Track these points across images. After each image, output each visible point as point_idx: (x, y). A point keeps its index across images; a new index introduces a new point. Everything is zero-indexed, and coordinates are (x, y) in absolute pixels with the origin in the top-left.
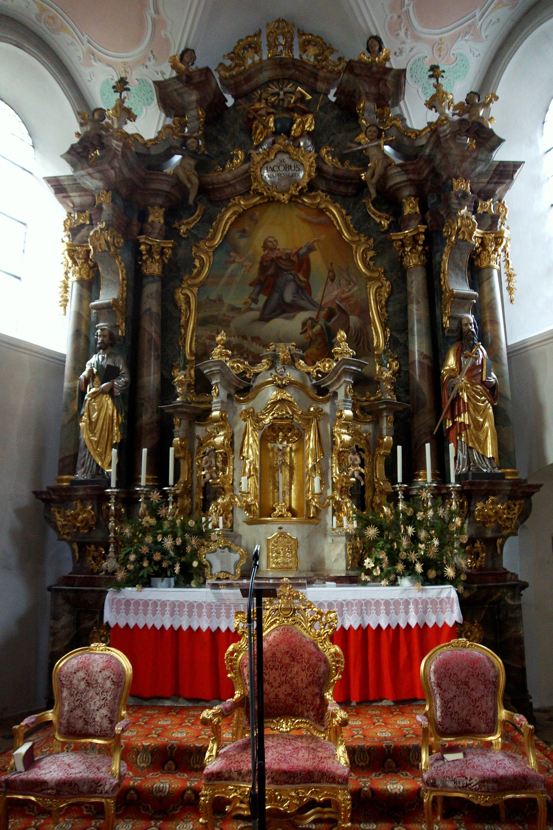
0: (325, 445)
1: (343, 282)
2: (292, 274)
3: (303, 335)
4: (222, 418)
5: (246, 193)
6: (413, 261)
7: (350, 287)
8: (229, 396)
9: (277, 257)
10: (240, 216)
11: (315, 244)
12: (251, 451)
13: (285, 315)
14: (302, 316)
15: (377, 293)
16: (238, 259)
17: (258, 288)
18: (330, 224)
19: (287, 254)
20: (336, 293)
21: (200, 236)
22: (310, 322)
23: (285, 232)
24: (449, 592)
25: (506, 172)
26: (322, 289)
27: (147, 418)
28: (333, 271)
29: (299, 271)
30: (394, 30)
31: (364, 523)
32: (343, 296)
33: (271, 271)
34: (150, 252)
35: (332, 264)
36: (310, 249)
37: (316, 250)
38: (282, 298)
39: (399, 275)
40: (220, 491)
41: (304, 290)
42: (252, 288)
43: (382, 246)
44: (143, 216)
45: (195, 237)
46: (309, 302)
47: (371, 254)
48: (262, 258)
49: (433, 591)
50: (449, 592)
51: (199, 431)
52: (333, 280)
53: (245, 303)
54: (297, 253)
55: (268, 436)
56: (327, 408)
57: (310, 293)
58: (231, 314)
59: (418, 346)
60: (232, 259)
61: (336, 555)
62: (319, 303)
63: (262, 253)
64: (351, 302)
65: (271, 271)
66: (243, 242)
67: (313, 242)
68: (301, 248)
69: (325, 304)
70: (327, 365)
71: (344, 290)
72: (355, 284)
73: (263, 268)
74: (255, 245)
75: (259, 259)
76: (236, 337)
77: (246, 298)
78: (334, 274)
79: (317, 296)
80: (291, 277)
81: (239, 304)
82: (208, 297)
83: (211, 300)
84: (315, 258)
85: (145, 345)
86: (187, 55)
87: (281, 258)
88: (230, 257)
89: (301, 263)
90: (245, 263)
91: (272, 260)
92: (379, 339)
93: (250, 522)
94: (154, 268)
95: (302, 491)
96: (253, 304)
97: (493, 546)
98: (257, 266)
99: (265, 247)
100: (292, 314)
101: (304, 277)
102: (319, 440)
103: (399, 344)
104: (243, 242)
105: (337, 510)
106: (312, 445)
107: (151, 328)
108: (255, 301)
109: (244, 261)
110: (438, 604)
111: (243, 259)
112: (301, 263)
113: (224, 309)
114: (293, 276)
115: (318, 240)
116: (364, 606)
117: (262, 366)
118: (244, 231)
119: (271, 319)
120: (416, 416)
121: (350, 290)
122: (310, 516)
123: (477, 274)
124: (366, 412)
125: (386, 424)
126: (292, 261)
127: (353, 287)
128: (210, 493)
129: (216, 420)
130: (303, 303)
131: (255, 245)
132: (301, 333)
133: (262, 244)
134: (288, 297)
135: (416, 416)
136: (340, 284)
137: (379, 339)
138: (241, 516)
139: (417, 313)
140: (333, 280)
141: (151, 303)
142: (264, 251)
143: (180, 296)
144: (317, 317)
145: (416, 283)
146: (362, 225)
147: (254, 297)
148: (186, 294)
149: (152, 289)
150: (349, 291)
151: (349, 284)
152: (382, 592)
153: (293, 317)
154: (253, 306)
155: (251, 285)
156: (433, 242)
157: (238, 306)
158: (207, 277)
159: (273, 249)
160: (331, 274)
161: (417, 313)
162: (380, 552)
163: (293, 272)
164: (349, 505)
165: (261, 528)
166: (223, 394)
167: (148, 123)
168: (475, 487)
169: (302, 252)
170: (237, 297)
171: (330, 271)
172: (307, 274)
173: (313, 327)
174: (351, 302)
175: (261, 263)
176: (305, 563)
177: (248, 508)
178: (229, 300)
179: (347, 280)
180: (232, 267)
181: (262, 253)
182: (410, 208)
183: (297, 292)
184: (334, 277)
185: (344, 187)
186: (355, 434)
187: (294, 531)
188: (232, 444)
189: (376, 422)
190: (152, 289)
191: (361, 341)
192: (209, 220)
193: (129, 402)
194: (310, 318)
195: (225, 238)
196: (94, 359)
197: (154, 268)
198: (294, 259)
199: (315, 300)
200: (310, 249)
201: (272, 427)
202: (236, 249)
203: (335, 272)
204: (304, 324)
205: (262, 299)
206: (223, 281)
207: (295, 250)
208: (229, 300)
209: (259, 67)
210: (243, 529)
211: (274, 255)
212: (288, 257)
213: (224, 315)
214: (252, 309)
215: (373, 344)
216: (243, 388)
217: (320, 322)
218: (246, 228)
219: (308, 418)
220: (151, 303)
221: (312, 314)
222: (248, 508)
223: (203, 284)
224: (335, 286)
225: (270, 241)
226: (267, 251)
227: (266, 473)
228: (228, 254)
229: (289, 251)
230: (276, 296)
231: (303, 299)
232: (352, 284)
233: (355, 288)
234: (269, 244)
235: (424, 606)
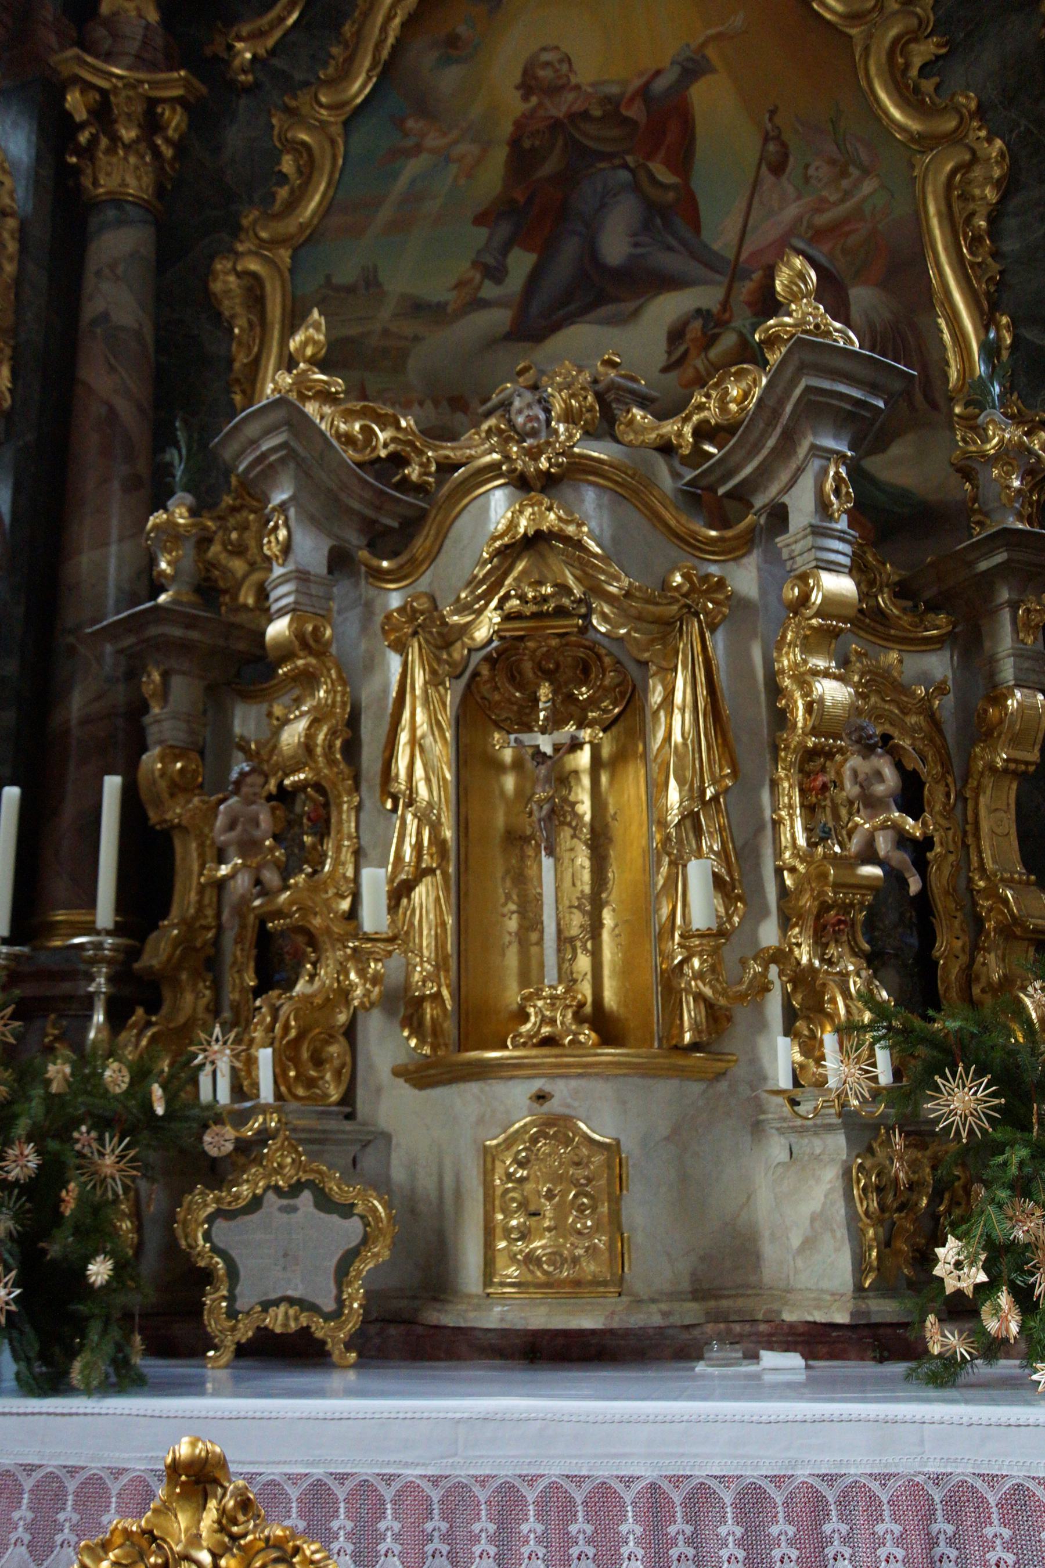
0: (744, 729)
1: (820, 170)
2: (625, 166)
3: (673, 376)
4: (305, 642)
7: (845, 183)
8: (340, 561)
9: (572, 117)
11: (711, 52)
13: (604, 311)
14: (668, 308)
15: (956, 195)
16: (433, 141)
17: (504, 229)
19: (607, 100)
20: (792, 211)
21: (299, 76)
22: (697, 324)
26: (741, 204)
28: (778, 138)
29: (649, 157)
31: (925, 1060)
32: (822, 220)
33: (549, 167)
34: (103, 113)
35: (773, 113)
36: (693, 69)
37: (712, 70)
38: (591, 251)
41: (673, 215)
42: (483, 232)
45: (285, 76)
46: (693, 255)
47: (923, 51)
48: (518, 125)
52: (778, 169)
53: (460, 285)
54: (644, 92)
55: (491, 695)
56: (745, 578)
57: (697, 227)
58: (409, 328)
60: (409, 143)
61: (806, 1222)
62: (730, 255)
63: (515, 105)
64: (852, 240)
65: (549, 167)
66: (449, 80)
67: (704, 45)
68: (658, 73)
69: (753, 255)
71: (823, 200)
72: (866, 172)
73: (522, 158)
75: (506, 129)
76: (429, 404)
77: (462, 268)
78: (784, 145)
80: (624, 175)
81: (437, 289)
82: (328, 278)
83: (338, 289)
84: (713, 101)
85: (89, 441)
87: (585, 115)
88: (406, 135)
89: (661, 122)
90: (462, 148)
91: (556, 125)
93: (421, 1076)
94: (122, 175)
95: (647, 929)
96: (487, 283)
98: (500, 154)
99: (528, 86)
100: (631, 306)
101: (675, 172)
102: (714, 711)
104: (449, 80)
105: (804, 1013)
106: (679, 726)
108: (496, 273)
109: (456, 142)
111: (455, 134)
112: (661, 122)
113: (385, 313)
114: (631, 171)
115: (720, 36)
118: (453, 41)
119: (555, 328)
121: (847, 195)
126: (626, 121)
127: (857, 184)
128: (277, 957)
129: (286, 654)
130: (673, 262)
131: (494, 89)
132: (665, 370)
133: (517, 77)
134: (615, 246)
136: (807, 179)
138: (386, 1046)
140: (778, 169)
142: (526, 98)
143: (225, 282)
144: (725, 305)
147: (490, 261)
149: (119, 247)
150: (842, 200)
151: (844, 174)
153: (636, 313)
154: (489, 291)
155: (480, 220)
157: (435, 299)
158: (327, 209)
159: (554, 90)
160: (772, 147)
163: (630, 159)
164: (853, 984)
165: (464, 1099)
166: (311, 550)
169: (660, 85)
171: (766, 139)
172: (683, 160)
173: (711, 341)
174: (852, 240)
175: (515, 143)
176: (658, 1260)
177: (405, 1006)
178: (400, 281)
179: (833, 162)
180: (413, 167)
181: (515, 105)
183: (646, 226)
184: (786, 156)
186: (876, 684)
187: (603, 1113)
188: (352, 749)
189: (970, 643)
190: (119, 247)
194: (699, 312)
195: (388, 72)
197: (122, 175)
198: (635, 112)
199: (716, 247)
200: (693, 69)
201: (505, 655)
202: (424, 107)
203: (785, 137)
204: (676, 335)
205: (521, 263)
206: (385, 213)
207: (637, 83)
208: (400, 281)
210: (395, 1106)
211: (560, 108)
212: (612, 109)
213: (386, 332)
214: (482, 304)
215: (946, 378)
216: (389, 519)
217: (737, 323)
218: (462, 30)
219: (664, 623)
220: (116, 294)
221: (704, 297)
222: (405, 1006)
223: (310, 239)
224: (791, 190)
225: (547, 64)
226: (534, 100)
228: (399, 123)
229: (615, 90)
230: (570, 249)
231: (670, 248)
232: (855, 172)
233: (868, 187)
234: (541, 73)
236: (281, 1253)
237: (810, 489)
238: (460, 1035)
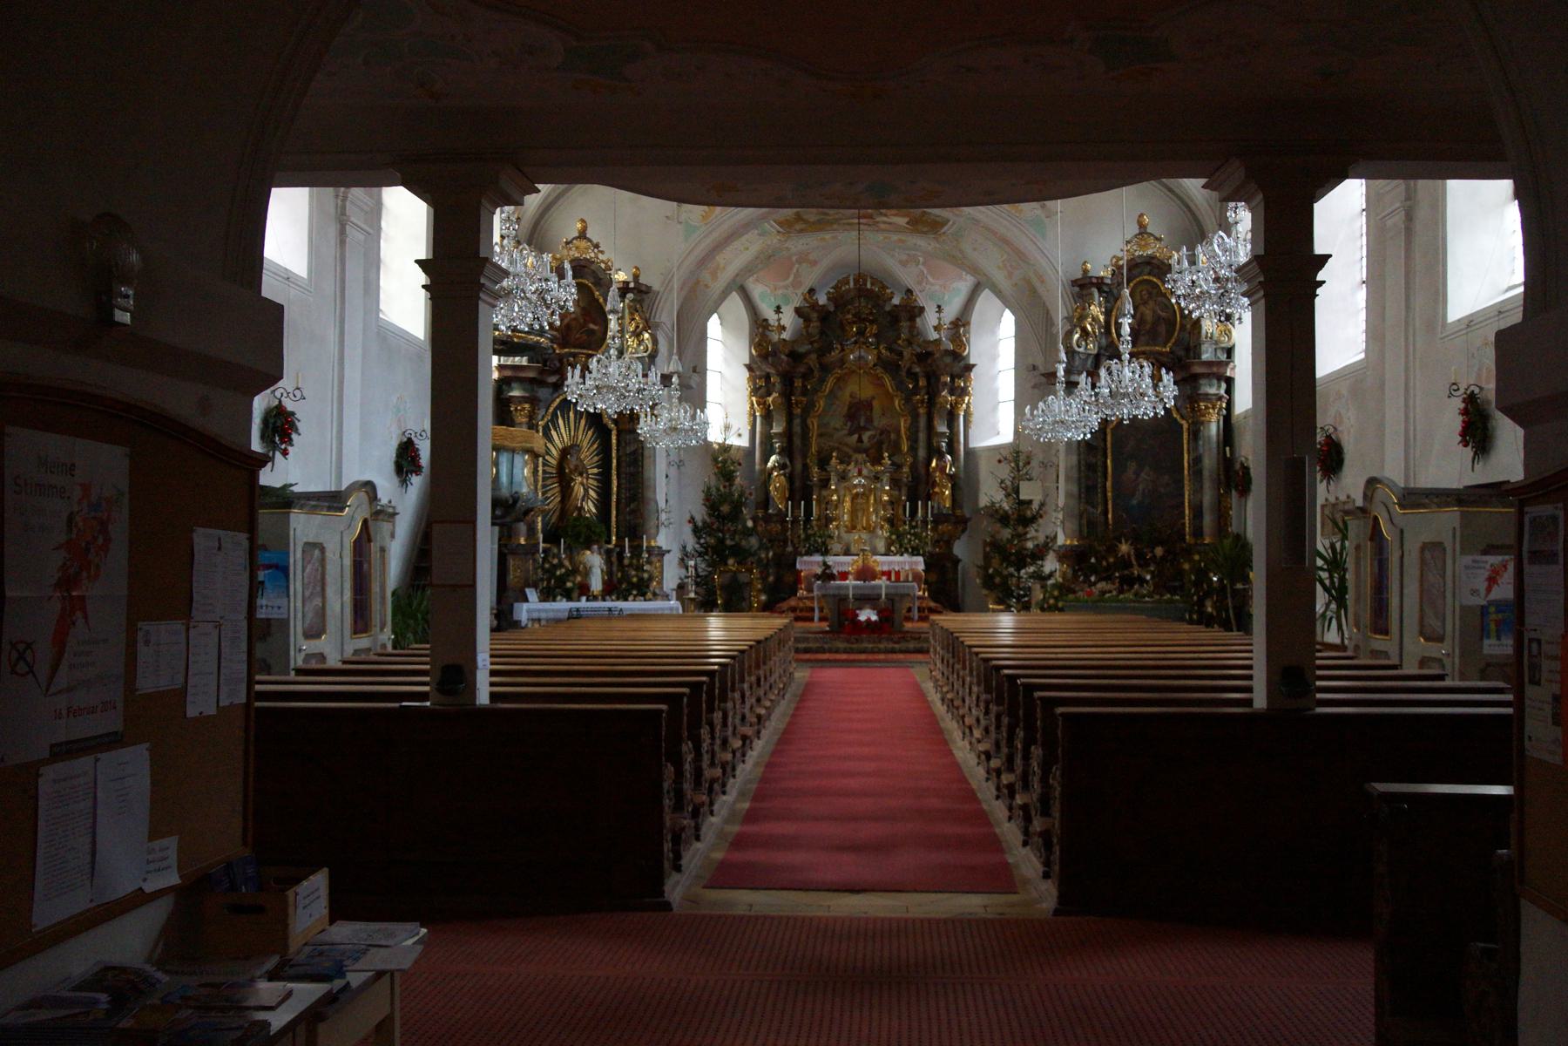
0: (878, 501)
5: (841, 367)
6: (921, 411)
10: (838, 379)
12: (847, 505)
18: (883, 385)
23: (860, 388)
24: (921, 559)
25: (969, 368)
27: (797, 484)
30: (920, 283)
39: (915, 417)
40: (835, 519)
41: (870, 420)
43: (908, 400)
44: (792, 383)
45: (815, 391)
49: (915, 558)
50: (921, 559)
51: (824, 493)
55: (855, 497)
59: (922, 453)
61: (881, 545)
70: (879, 468)
74: (845, 396)
79: (876, 423)
84: (876, 404)
86: (812, 291)
92: (905, 448)
97: (949, 544)
103: (913, 449)
107: (797, 442)
110: (917, 563)
116: (890, 563)
117: (851, 467)
120: (918, 487)
122: (870, 529)
123: (951, 418)
124: (895, 483)
125: (904, 491)
131: (845, 396)
135: (918, 487)
137: (905, 448)
139: (922, 436)
141: (797, 429)
145: (922, 422)
146: (900, 386)
148: (813, 423)
149: (797, 421)
152: (898, 558)
156: (931, 403)
161: (922, 436)
162: (898, 543)
167: (788, 318)
168: (939, 518)
170: (837, 422)
182: (922, 382)
185: (891, 367)
187: (865, 536)
190: (797, 421)
191: (895, 449)
192: (822, 380)
193: (790, 478)
196: (773, 458)
197: (798, 411)
209: (849, 290)
210: (844, 535)
216: (843, 477)
220: (797, 429)
227: (853, 512)
235: (911, 563)
236: (836, 547)
237: (886, 478)
238: (852, 528)
